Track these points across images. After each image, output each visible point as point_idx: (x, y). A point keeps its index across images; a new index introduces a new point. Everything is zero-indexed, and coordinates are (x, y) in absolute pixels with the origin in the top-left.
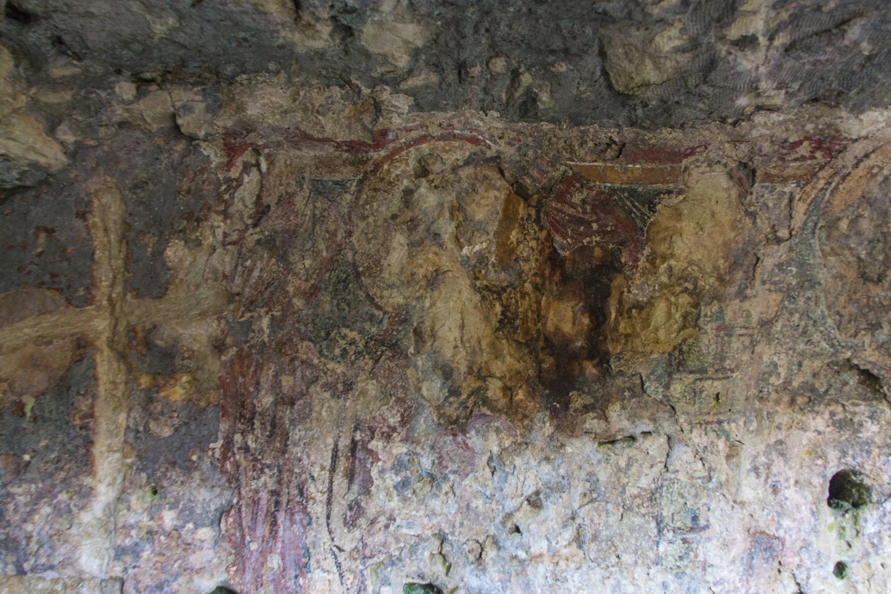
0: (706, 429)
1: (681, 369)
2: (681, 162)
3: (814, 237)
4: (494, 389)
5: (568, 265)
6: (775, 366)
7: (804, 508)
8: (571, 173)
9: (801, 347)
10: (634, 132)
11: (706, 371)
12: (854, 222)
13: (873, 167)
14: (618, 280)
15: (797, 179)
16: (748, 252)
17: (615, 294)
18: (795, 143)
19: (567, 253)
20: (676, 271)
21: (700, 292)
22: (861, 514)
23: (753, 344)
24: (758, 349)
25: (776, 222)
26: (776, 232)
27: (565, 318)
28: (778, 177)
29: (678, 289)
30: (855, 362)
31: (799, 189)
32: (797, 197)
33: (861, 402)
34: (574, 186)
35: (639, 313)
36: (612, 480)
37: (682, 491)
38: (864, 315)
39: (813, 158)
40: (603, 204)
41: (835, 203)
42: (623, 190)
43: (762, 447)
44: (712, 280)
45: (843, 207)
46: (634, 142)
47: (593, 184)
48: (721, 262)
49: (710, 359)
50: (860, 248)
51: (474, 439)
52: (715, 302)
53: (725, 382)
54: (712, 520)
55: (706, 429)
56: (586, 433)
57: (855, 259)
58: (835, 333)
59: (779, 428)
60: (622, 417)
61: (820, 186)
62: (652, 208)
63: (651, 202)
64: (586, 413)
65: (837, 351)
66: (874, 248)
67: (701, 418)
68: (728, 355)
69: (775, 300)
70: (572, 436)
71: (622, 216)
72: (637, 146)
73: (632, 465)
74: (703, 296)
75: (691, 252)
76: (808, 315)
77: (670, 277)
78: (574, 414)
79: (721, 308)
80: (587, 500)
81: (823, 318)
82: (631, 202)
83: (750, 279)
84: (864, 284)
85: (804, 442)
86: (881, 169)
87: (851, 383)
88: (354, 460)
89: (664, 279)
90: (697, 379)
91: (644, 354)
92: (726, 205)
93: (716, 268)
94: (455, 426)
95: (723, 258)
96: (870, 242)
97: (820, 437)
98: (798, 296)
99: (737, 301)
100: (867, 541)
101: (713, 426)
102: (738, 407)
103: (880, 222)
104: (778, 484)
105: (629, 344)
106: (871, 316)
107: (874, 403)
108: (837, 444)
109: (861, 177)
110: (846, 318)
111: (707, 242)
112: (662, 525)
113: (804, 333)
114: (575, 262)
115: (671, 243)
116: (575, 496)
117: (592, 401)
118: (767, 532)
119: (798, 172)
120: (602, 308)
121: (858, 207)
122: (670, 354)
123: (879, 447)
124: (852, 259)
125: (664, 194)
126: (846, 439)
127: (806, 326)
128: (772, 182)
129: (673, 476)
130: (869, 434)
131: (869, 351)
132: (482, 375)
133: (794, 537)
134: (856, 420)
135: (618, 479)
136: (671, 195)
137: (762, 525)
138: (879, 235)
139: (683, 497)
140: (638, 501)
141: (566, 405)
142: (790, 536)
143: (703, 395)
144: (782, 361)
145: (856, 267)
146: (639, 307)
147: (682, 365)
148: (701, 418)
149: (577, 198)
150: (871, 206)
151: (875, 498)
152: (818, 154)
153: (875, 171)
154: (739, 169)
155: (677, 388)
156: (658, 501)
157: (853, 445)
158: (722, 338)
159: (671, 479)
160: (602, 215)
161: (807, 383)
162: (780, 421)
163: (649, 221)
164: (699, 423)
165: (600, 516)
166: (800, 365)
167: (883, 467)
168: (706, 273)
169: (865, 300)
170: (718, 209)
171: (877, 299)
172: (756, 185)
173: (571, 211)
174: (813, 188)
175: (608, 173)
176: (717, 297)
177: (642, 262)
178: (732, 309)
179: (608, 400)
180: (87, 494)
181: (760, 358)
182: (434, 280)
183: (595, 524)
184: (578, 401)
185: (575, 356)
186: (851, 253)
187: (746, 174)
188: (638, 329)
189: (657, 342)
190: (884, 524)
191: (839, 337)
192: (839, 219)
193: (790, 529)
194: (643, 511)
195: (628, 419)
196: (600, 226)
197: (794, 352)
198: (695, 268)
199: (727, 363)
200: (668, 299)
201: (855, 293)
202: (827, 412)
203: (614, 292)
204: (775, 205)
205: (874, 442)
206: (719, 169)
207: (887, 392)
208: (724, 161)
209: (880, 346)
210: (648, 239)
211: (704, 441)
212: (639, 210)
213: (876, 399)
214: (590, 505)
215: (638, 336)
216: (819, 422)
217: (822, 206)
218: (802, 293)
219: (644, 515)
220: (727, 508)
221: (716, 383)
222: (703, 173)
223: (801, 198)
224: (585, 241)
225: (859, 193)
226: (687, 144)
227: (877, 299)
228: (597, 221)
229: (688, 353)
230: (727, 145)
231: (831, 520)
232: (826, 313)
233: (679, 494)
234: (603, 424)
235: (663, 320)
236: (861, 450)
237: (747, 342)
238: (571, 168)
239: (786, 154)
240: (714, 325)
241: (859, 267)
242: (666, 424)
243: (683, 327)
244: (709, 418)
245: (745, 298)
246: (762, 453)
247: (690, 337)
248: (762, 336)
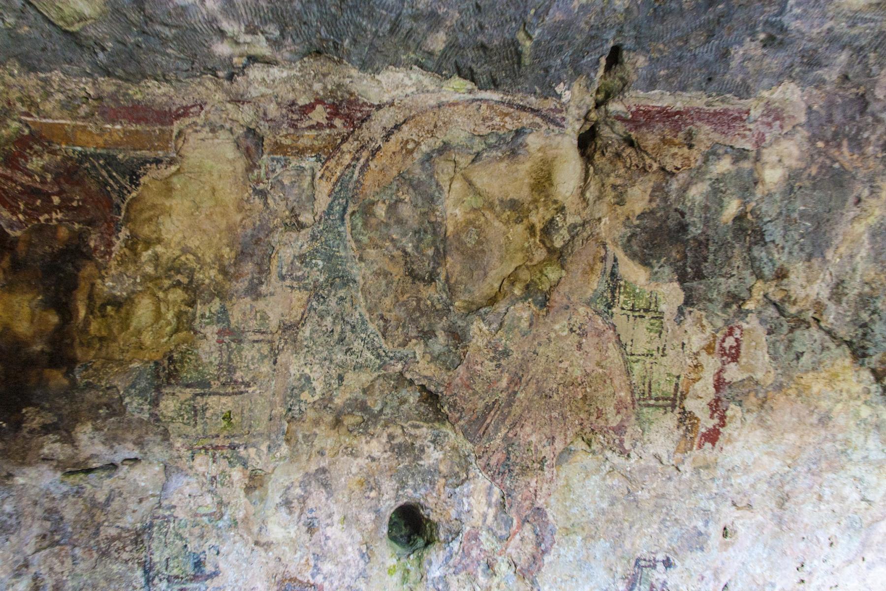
0: (214, 456)
1: (173, 381)
2: (172, 124)
3: (343, 224)
5: (21, 248)
6: (308, 379)
7: (350, 549)
8: (27, 131)
9: (339, 357)
10: (115, 84)
11: (209, 385)
12: (392, 208)
13: (407, 142)
14: (88, 269)
15: (317, 152)
16: (260, 239)
17: (84, 286)
18: (306, 106)
19: (18, 233)
20: (164, 260)
21: (198, 287)
22: (425, 555)
23: (274, 353)
24: (281, 359)
25: (295, 204)
26: (296, 216)
28: (292, 148)
29: (167, 283)
30: (408, 376)
31: (320, 164)
32: (319, 175)
33: (422, 423)
34: (31, 148)
35: (117, 311)
36: (83, 518)
37: (181, 531)
38: (413, 320)
39: (332, 126)
40: (70, 173)
41: (367, 183)
42: (97, 157)
43: (298, 476)
44: (213, 273)
45: (377, 189)
46: (113, 97)
47: (58, 147)
48: (226, 251)
49: (213, 370)
50: (404, 241)
52: (217, 300)
53: (237, 398)
54: (222, 565)
55: (214, 456)
56: (44, 459)
57: (400, 253)
58: (380, 341)
59: (321, 453)
60: (96, 441)
61: (346, 162)
62: (134, 179)
63: (134, 173)
64: (46, 434)
65: (385, 363)
66: (420, 240)
67: (206, 442)
68: (239, 365)
69: (299, 300)
70: (22, 464)
71: (94, 188)
72: (117, 101)
73: (113, 500)
74: (201, 292)
75: (184, 237)
76: (343, 319)
77: (156, 267)
78: (28, 436)
79: (223, 307)
80: (47, 543)
81: (363, 323)
82: (108, 171)
83: (263, 270)
84: (414, 283)
85: (354, 470)
86: (418, 144)
87: (411, 400)
89: (149, 269)
90: (197, 395)
91: (120, 363)
92: (231, 180)
93: (219, 258)
95: (228, 246)
96: (415, 232)
97: (374, 464)
98: (328, 296)
99: (248, 299)
100: (431, 586)
101: (225, 451)
102: (262, 427)
103: (426, 210)
104: (315, 522)
105: (104, 349)
106: (423, 322)
107: (437, 425)
108: (393, 473)
109: (394, 153)
110: (393, 323)
111: (207, 225)
112: (151, 573)
113: (341, 340)
114: (30, 244)
115: (158, 224)
117: (56, 419)
118: (300, 578)
119: (316, 143)
120: (66, 304)
121: (398, 190)
122: (156, 363)
123: (445, 477)
124: (396, 253)
125: (151, 163)
126: (406, 467)
127: (343, 332)
128: (285, 154)
129: (168, 513)
130: (431, 462)
131: (422, 364)
133: (336, 583)
134: (417, 444)
135: (93, 516)
136: (160, 166)
137: (292, 570)
138: (426, 224)
139: (182, 539)
140: (118, 544)
141: (17, 426)
142: (331, 583)
143: (208, 414)
144: (317, 374)
145: (403, 262)
146: (117, 303)
147: (174, 377)
148: (206, 442)
149: (35, 164)
150: (415, 190)
151: (442, 536)
152: (338, 122)
153: (410, 146)
154: (246, 137)
155: (169, 405)
156: (146, 544)
157: (413, 474)
158: (228, 346)
159: (165, 517)
160: (66, 187)
161: (356, 400)
162: (323, 445)
163: (129, 197)
164: (204, 448)
165: (63, 563)
166: (341, 378)
167: (448, 500)
168: (205, 264)
169: (415, 303)
170: (220, 185)
171: (429, 302)
172: (265, 156)
173: (25, 179)
174: (337, 164)
175: (79, 133)
176: (221, 294)
177: (118, 245)
178: (240, 310)
179: (76, 419)
181: (287, 369)
183: (56, 574)
184: (34, 419)
185: (31, 362)
186: (395, 246)
187: (252, 143)
188: (115, 331)
189: (141, 347)
190: (450, 567)
191: (384, 346)
192: (373, 203)
193: (331, 575)
194: (125, 556)
195: (103, 443)
196: (62, 200)
197: (331, 361)
198: (191, 257)
199: (238, 375)
200: (154, 295)
201: (402, 293)
202: (385, 435)
203: (83, 284)
204: (293, 183)
205: (437, 471)
206: (223, 135)
207: (448, 412)
208: (228, 126)
209: (435, 359)
210: (127, 219)
211: (214, 469)
212: (117, 182)
213: (438, 420)
214: (48, 550)
215: (115, 340)
216: (375, 447)
217: (351, 186)
218: (333, 293)
219: (126, 562)
220: (245, 552)
221: (224, 400)
222: (203, 140)
223: (323, 176)
224: (42, 219)
225: (395, 173)
226: (179, 102)
227: (429, 302)
228: (58, 194)
229: (181, 361)
230: (229, 106)
231: (391, 562)
232: (367, 317)
233: (177, 535)
234: (69, 450)
235: (150, 321)
236: (423, 481)
237: (266, 349)
238: (27, 126)
239: (297, 120)
240: (216, 328)
241: (406, 263)
242: (157, 449)
243: (177, 331)
244: (219, 442)
245: (258, 296)
246: (297, 484)
247: (184, 341)
248: (286, 343)
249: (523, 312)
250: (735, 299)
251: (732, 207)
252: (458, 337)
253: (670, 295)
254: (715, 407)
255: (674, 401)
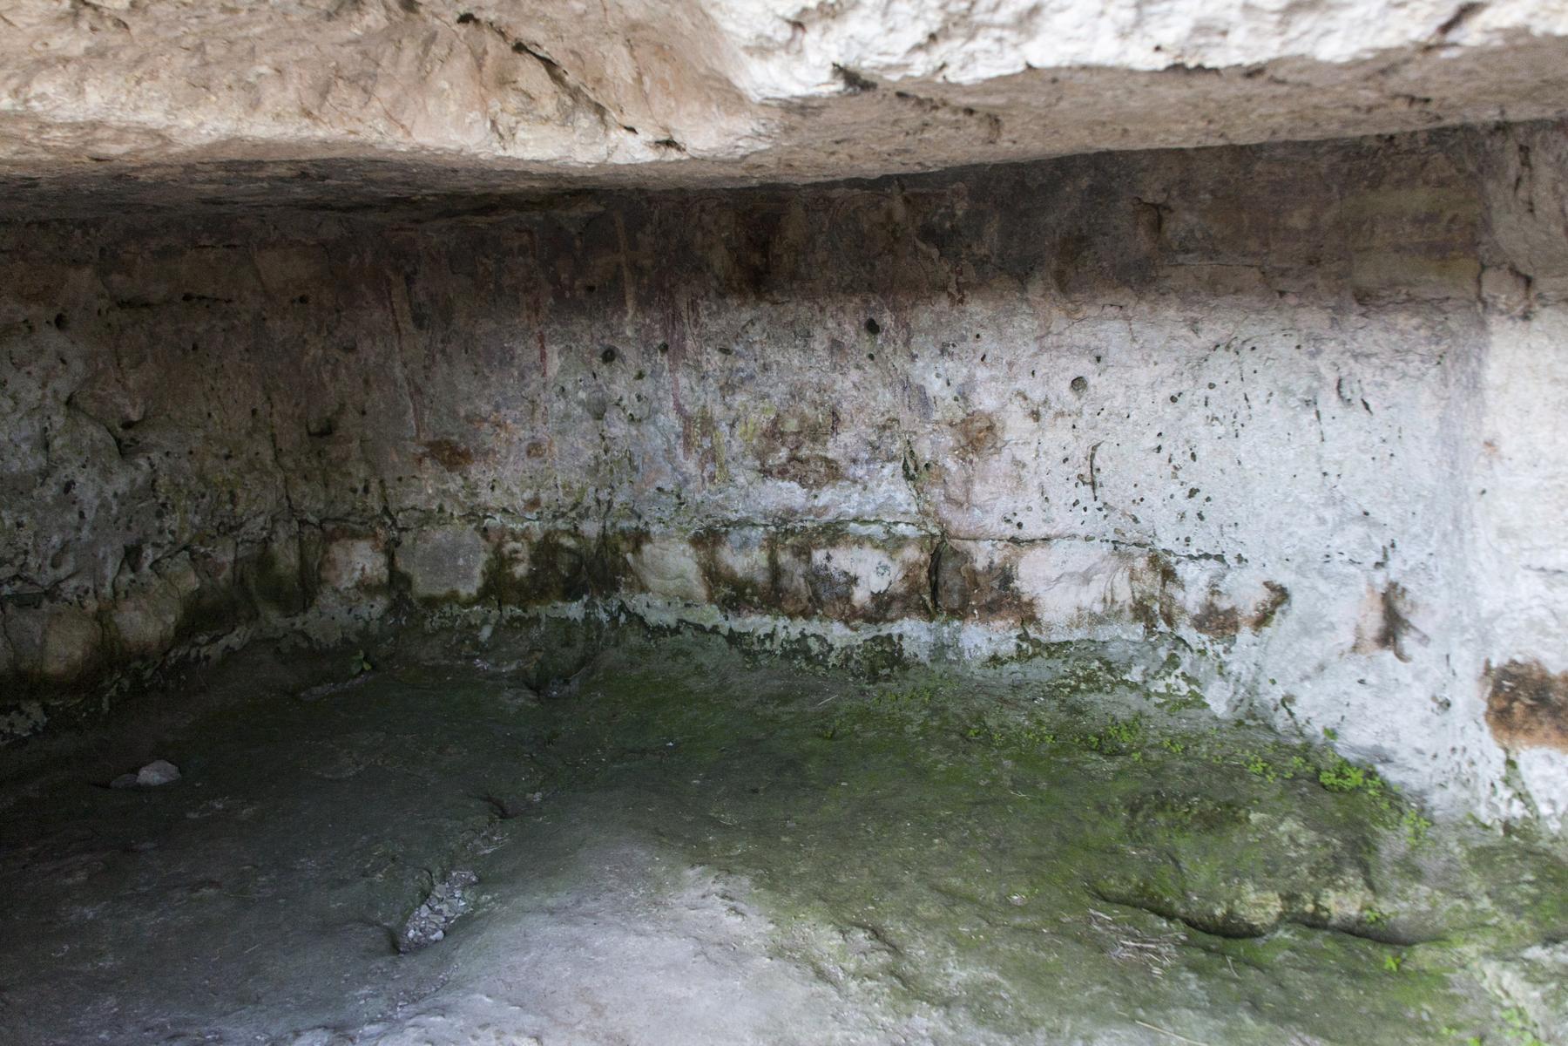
4: (735, 284)
27: (756, 259)
51: (728, 301)
88: (693, 306)
94: (722, 296)
116: (765, 320)
132: (729, 279)
180: (626, 313)
182: (711, 247)
216: (857, 300)
249: (890, 258)
250: (957, 254)
251: (948, 225)
252: (873, 266)
253: (935, 252)
254: (959, 291)
255: (944, 288)
